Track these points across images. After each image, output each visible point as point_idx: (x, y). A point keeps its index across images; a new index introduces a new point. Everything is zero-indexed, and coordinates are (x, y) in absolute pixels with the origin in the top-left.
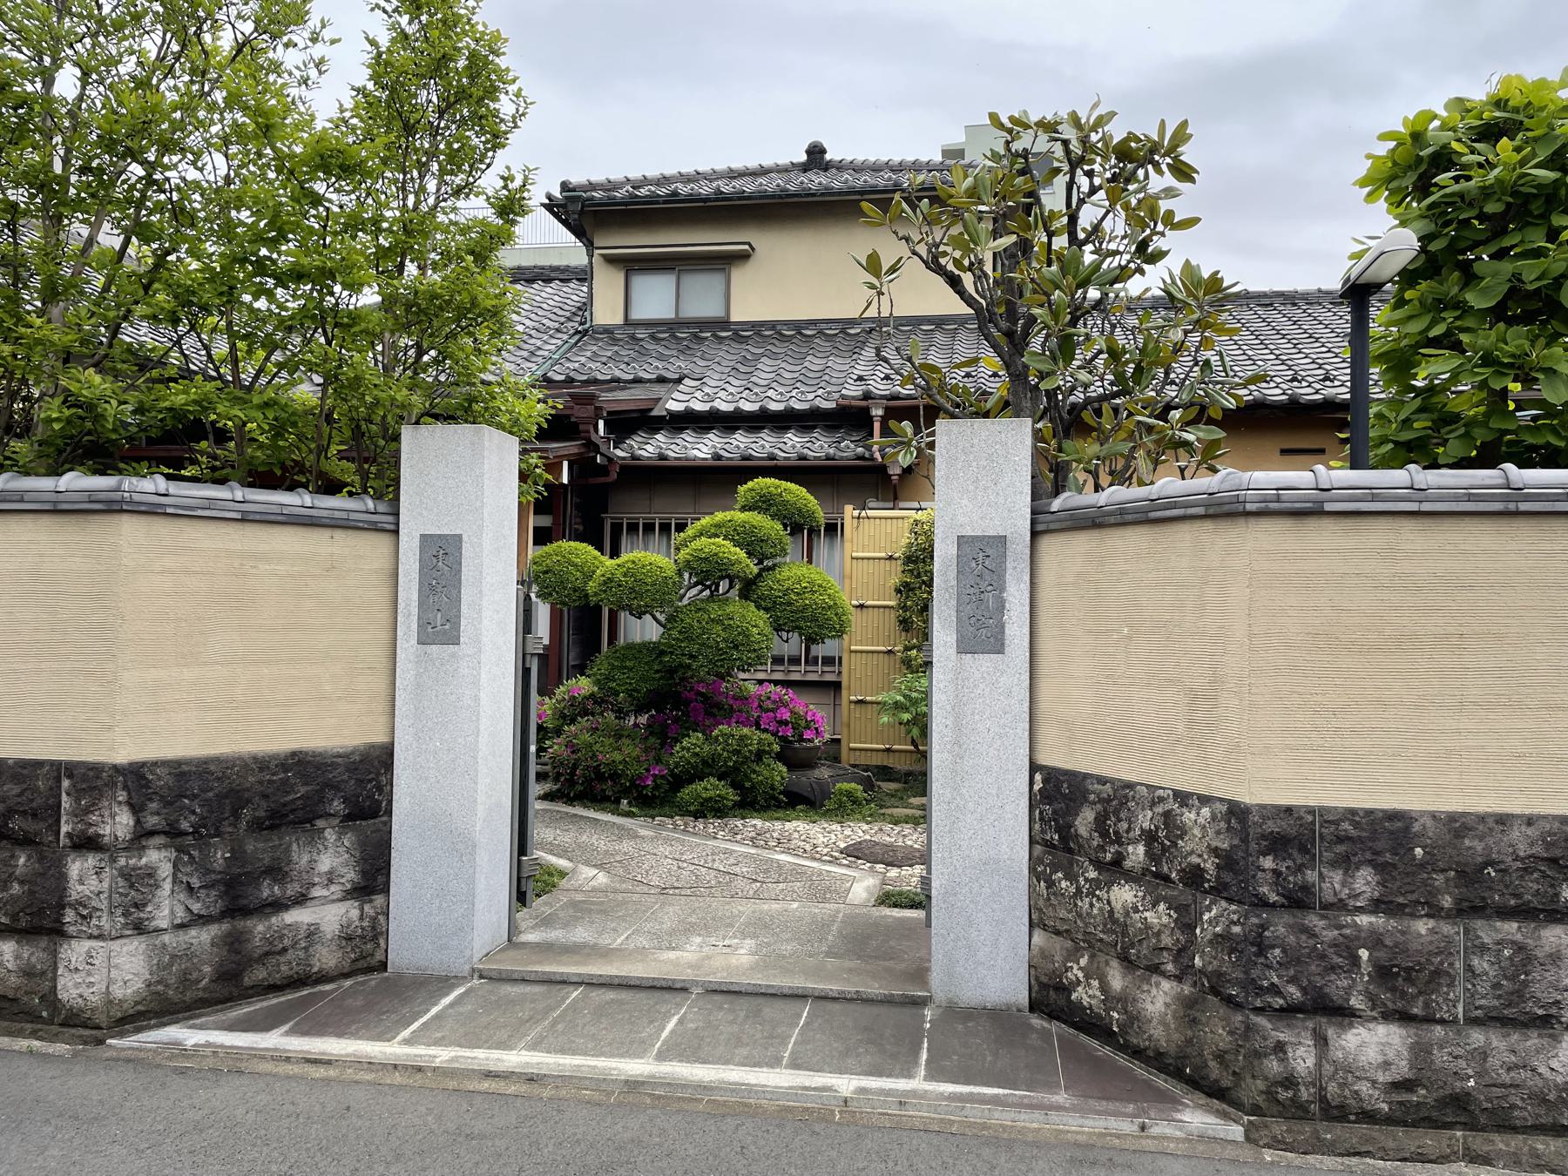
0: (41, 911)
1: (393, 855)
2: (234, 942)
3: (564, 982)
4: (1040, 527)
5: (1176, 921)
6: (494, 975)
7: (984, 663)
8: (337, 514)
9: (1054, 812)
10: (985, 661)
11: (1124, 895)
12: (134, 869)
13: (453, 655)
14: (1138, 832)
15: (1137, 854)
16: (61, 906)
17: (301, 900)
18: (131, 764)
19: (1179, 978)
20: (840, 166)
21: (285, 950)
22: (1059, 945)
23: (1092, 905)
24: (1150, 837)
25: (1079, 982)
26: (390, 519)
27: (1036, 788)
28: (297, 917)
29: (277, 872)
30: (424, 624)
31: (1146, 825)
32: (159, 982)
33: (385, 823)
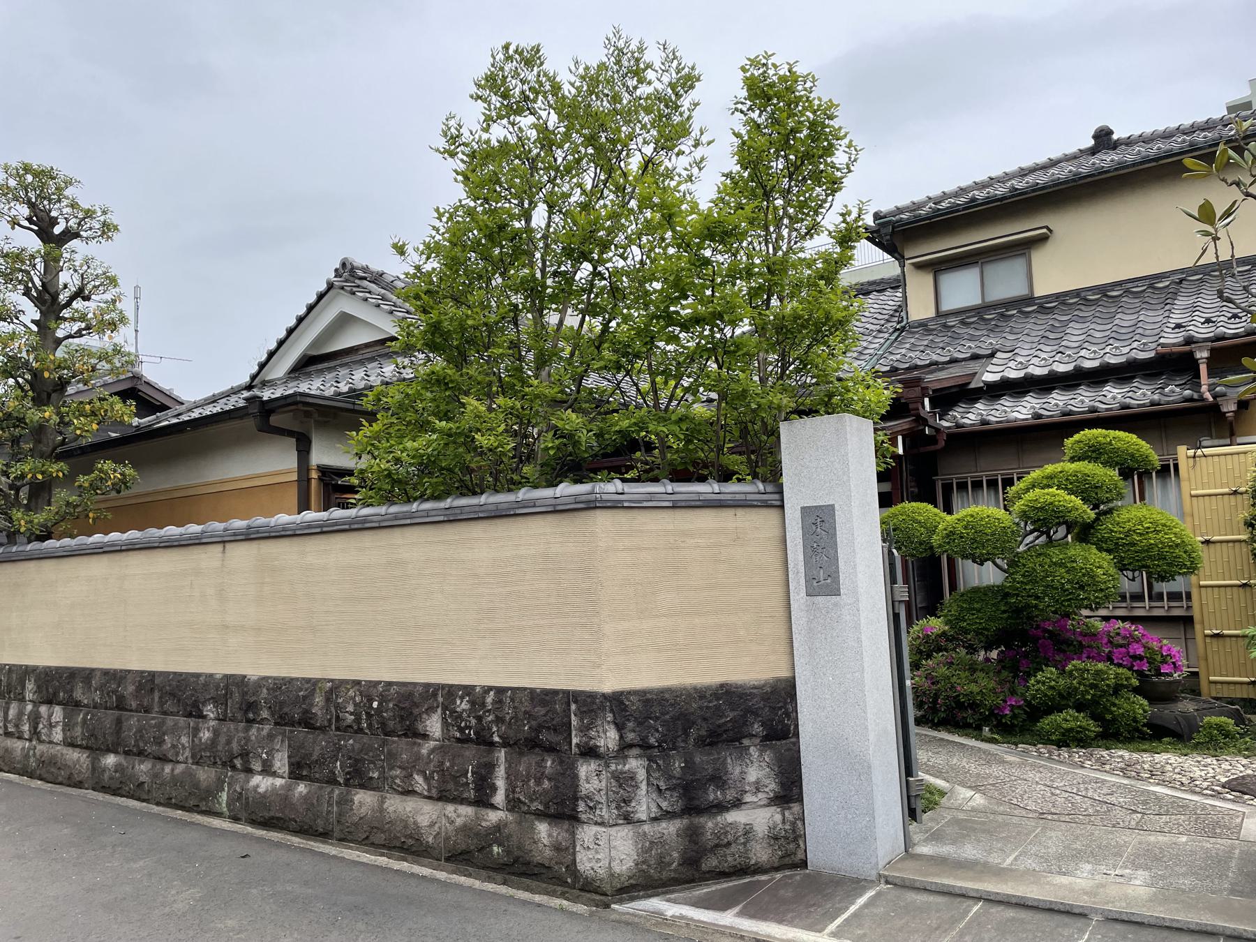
0: (562, 803)
2: (692, 834)
3: (963, 895)
6: (897, 881)
13: (836, 605)
16: (577, 799)
17: (738, 804)
18: (614, 693)
20: (1129, 142)
21: (729, 844)
26: (777, 496)
28: (734, 817)
29: (719, 779)
30: (810, 579)
33: (794, 744)
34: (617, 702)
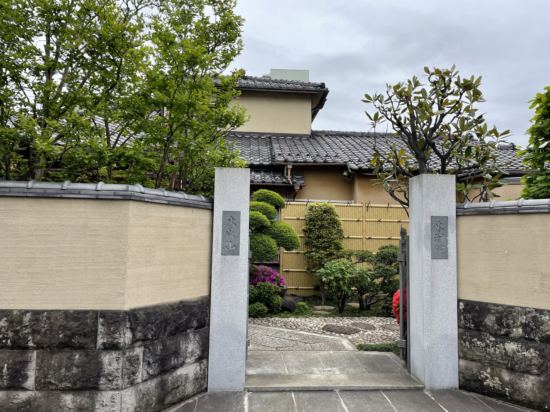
0: (88, 380)
1: (210, 342)
2: (162, 385)
3: (283, 391)
4: (459, 214)
5: (539, 355)
6: (254, 390)
7: (441, 263)
8: (196, 202)
9: (473, 317)
10: (441, 262)
11: (511, 347)
12: (132, 357)
13: (236, 260)
14: (519, 324)
15: (519, 331)
16: (99, 376)
17: (182, 364)
18: (131, 310)
19: (538, 375)
20: (251, 78)
21: (178, 387)
22: (474, 366)
23: (495, 350)
24: (525, 326)
25: (487, 378)
26: (210, 204)
27: (461, 308)
28: (181, 372)
29: (176, 353)
30: (224, 247)
31: (524, 321)
32: (139, 407)
33: (206, 329)
34: (132, 316)
